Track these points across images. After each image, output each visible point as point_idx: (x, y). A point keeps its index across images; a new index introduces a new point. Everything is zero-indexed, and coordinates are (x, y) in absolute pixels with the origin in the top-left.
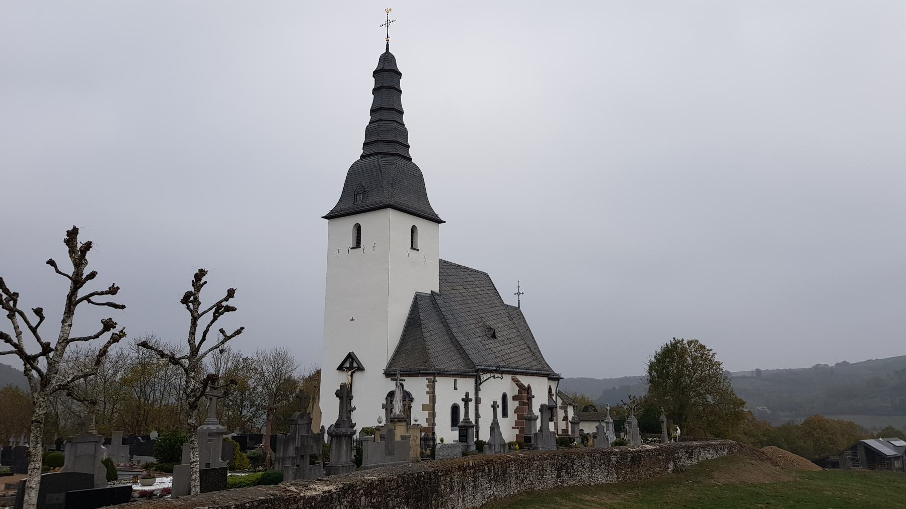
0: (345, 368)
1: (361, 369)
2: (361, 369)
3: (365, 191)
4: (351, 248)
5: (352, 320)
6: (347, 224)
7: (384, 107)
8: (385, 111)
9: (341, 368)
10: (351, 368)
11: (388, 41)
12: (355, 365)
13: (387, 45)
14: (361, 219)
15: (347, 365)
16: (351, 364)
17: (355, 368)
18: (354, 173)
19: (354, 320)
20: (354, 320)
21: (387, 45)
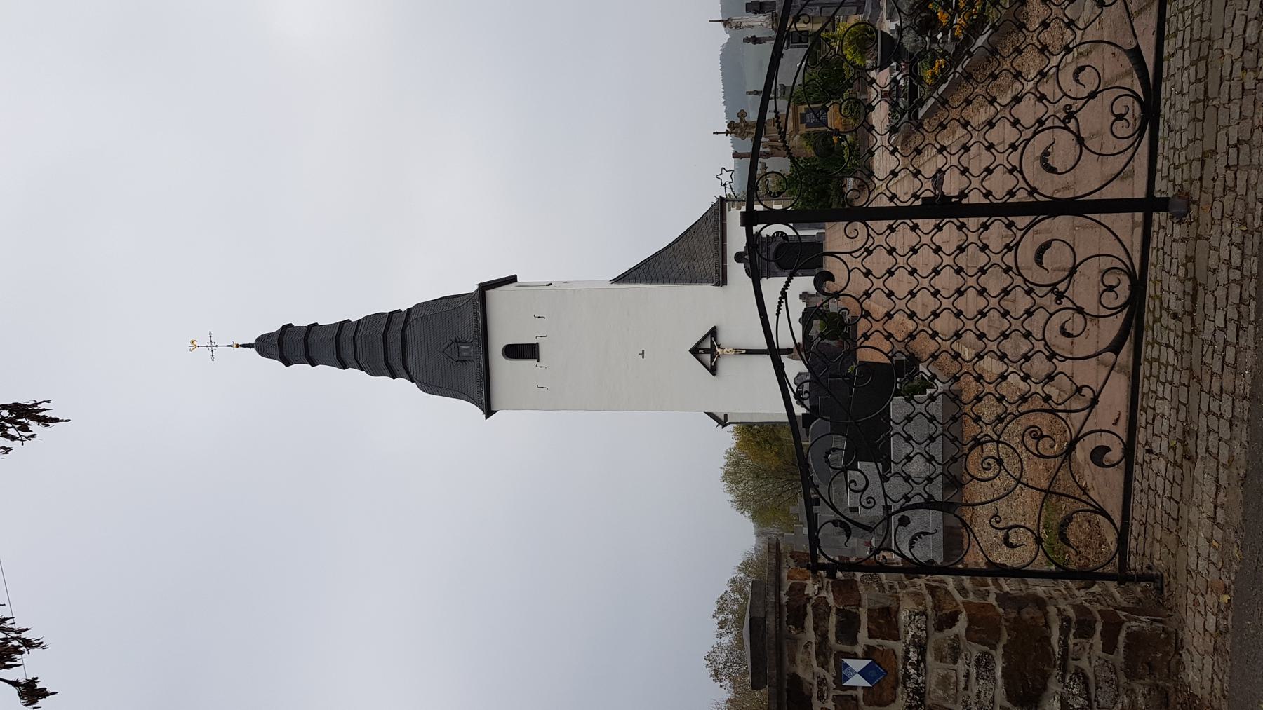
0: (712, 361)
1: (713, 333)
2: (713, 333)
3: (456, 341)
4: (538, 361)
5: (643, 354)
6: (504, 371)
7: (335, 334)
8: (342, 333)
9: (713, 370)
10: (712, 351)
11: (237, 346)
12: (707, 345)
13: (244, 346)
14: (498, 343)
15: (707, 357)
16: (706, 351)
17: (712, 342)
18: (429, 386)
19: (643, 351)
20: (643, 351)
21: (244, 346)
